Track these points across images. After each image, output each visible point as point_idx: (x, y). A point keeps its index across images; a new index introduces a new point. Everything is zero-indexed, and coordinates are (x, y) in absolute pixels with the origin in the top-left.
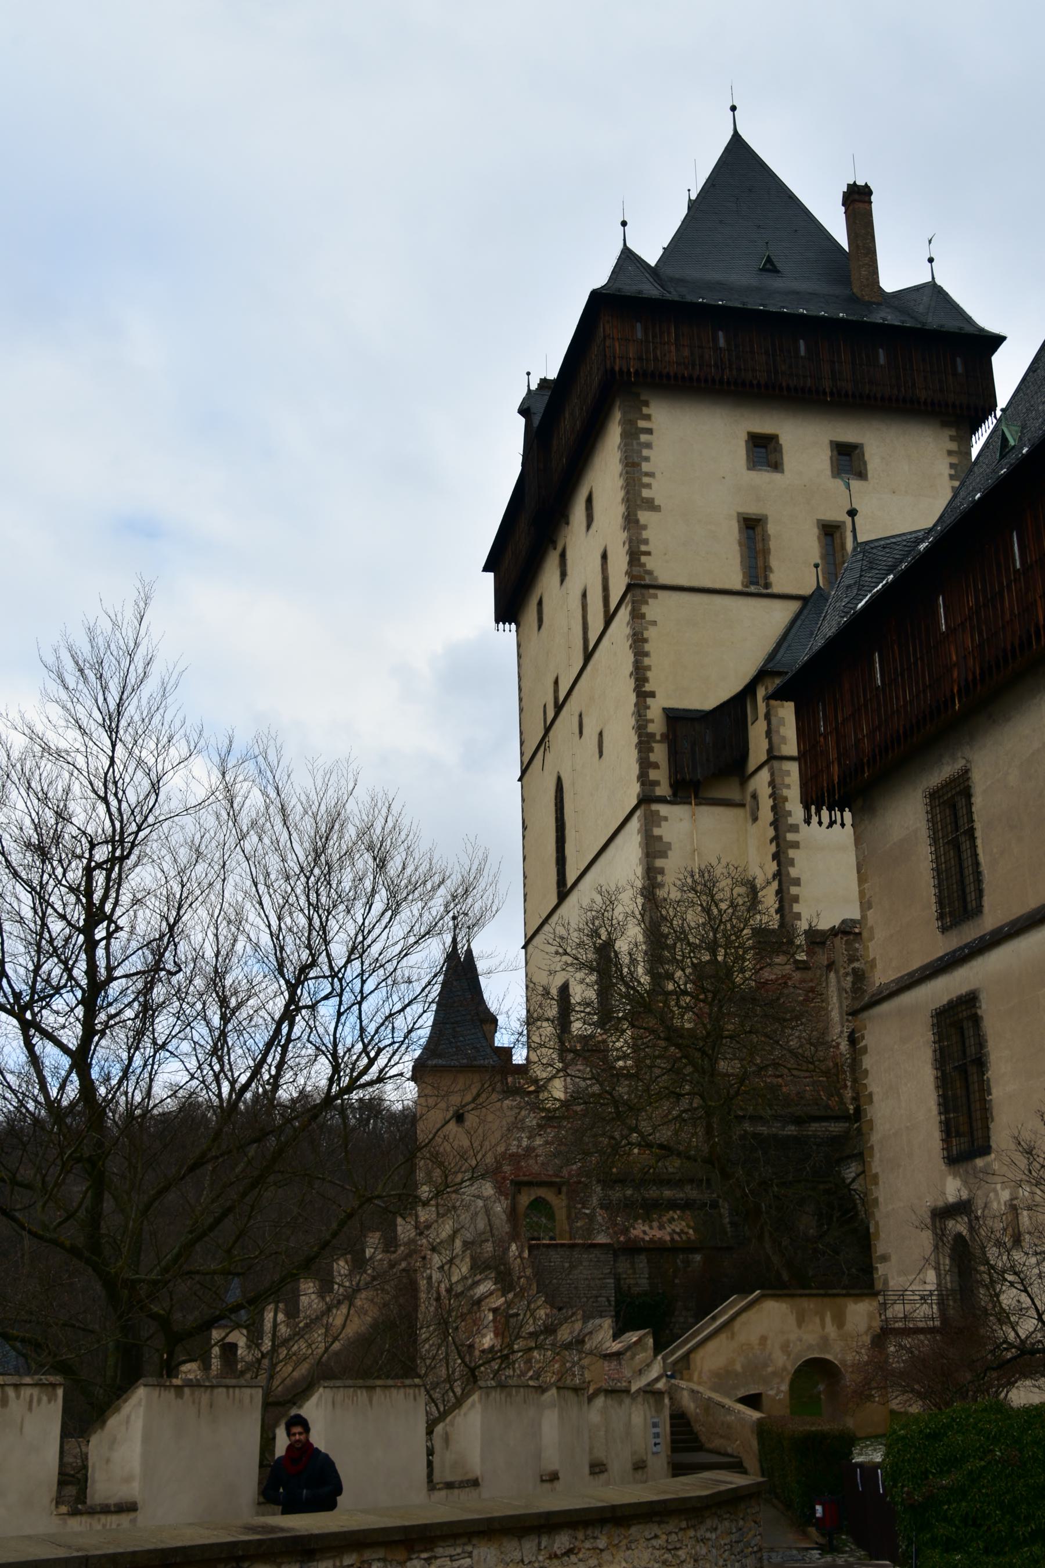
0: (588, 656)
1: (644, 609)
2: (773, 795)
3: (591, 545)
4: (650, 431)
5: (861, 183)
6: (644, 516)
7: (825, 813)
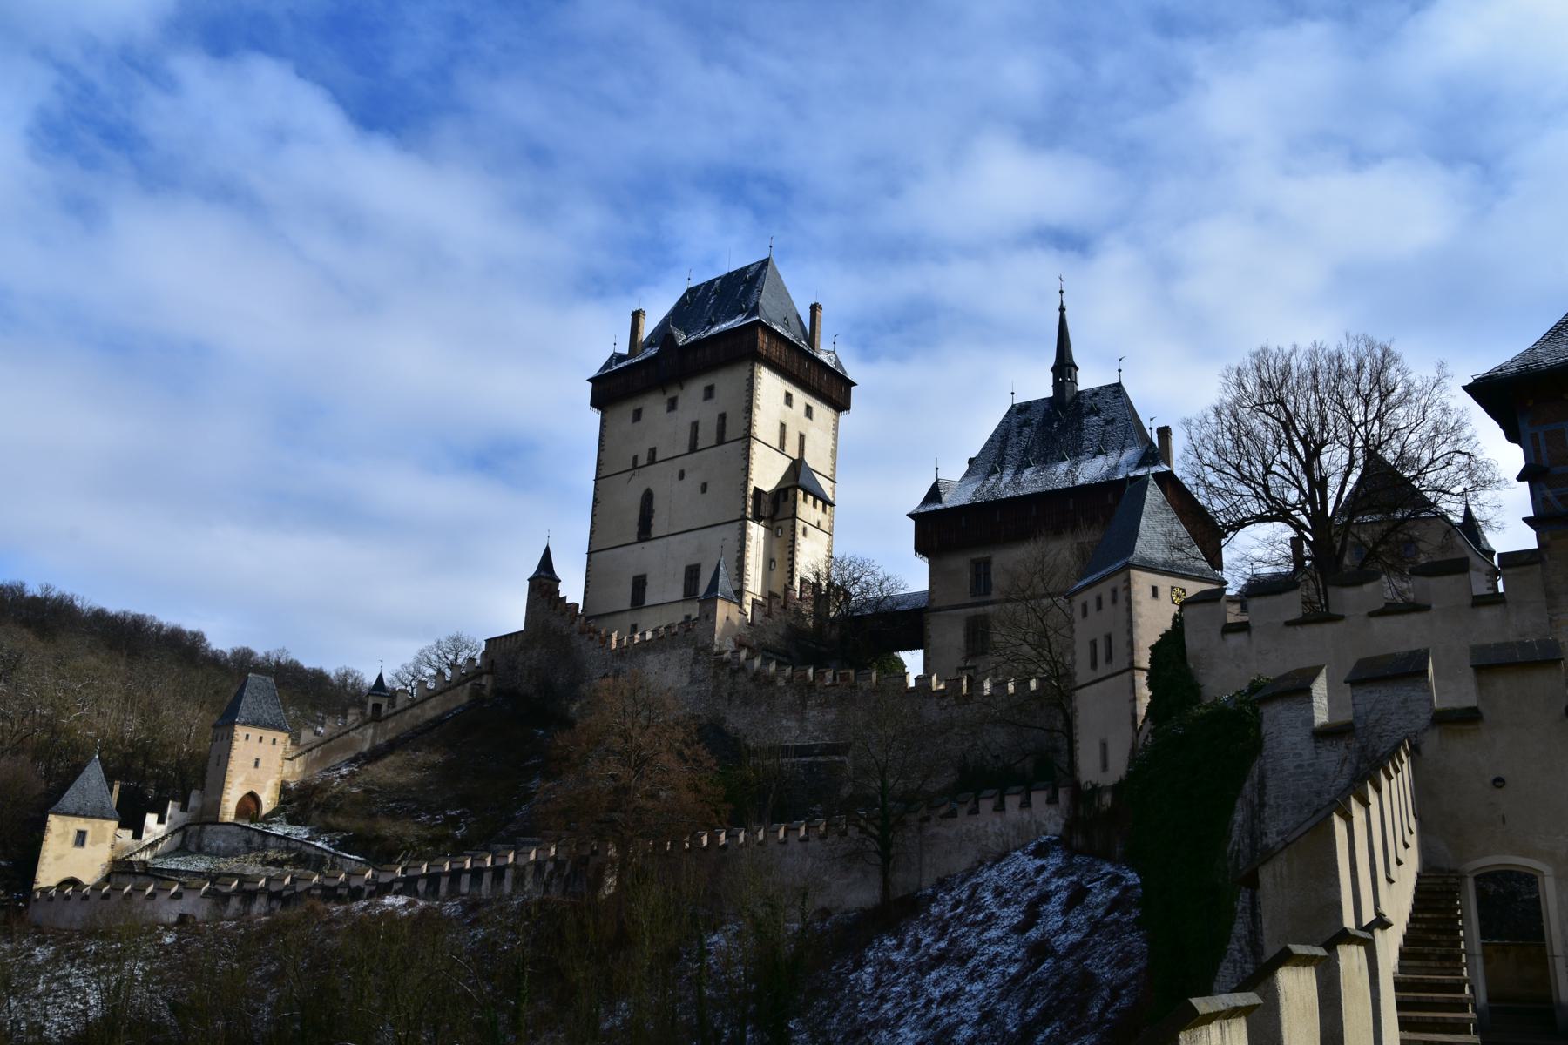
0: (693, 448)
6: (756, 411)
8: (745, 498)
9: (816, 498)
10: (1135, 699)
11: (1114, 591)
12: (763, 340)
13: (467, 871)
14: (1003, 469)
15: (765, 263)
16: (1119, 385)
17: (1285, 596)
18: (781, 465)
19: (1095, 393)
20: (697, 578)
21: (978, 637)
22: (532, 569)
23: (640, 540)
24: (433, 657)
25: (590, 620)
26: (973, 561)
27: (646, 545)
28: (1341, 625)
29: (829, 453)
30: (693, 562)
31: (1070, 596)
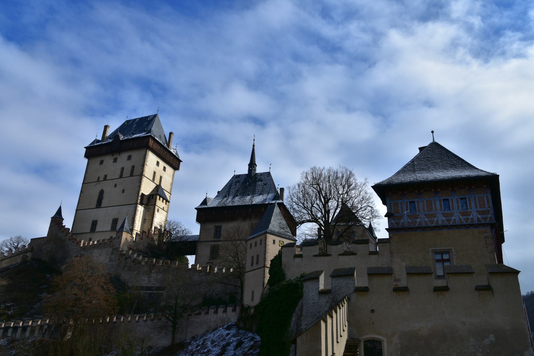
0: (121, 177)
6: (146, 166)
8: (138, 196)
9: (163, 199)
10: (264, 277)
11: (261, 240)
12: (151, 142)
13: (12, 328)
14: (229, 196)
15: (155, 116)
16: (269, 173)
17: (314, 247)
18: (153, 186)
19: (261, 174)
20: (117, 223)
21: (214, 253)
22: (53, 213)
23: (97, 207)
24: (8, 244)
25: (73, 235)
26: (215, 226)
27: (99, 209)
28: (330, 257)
29: (170, 184)
30: (116, 217)
31: (246, 241)
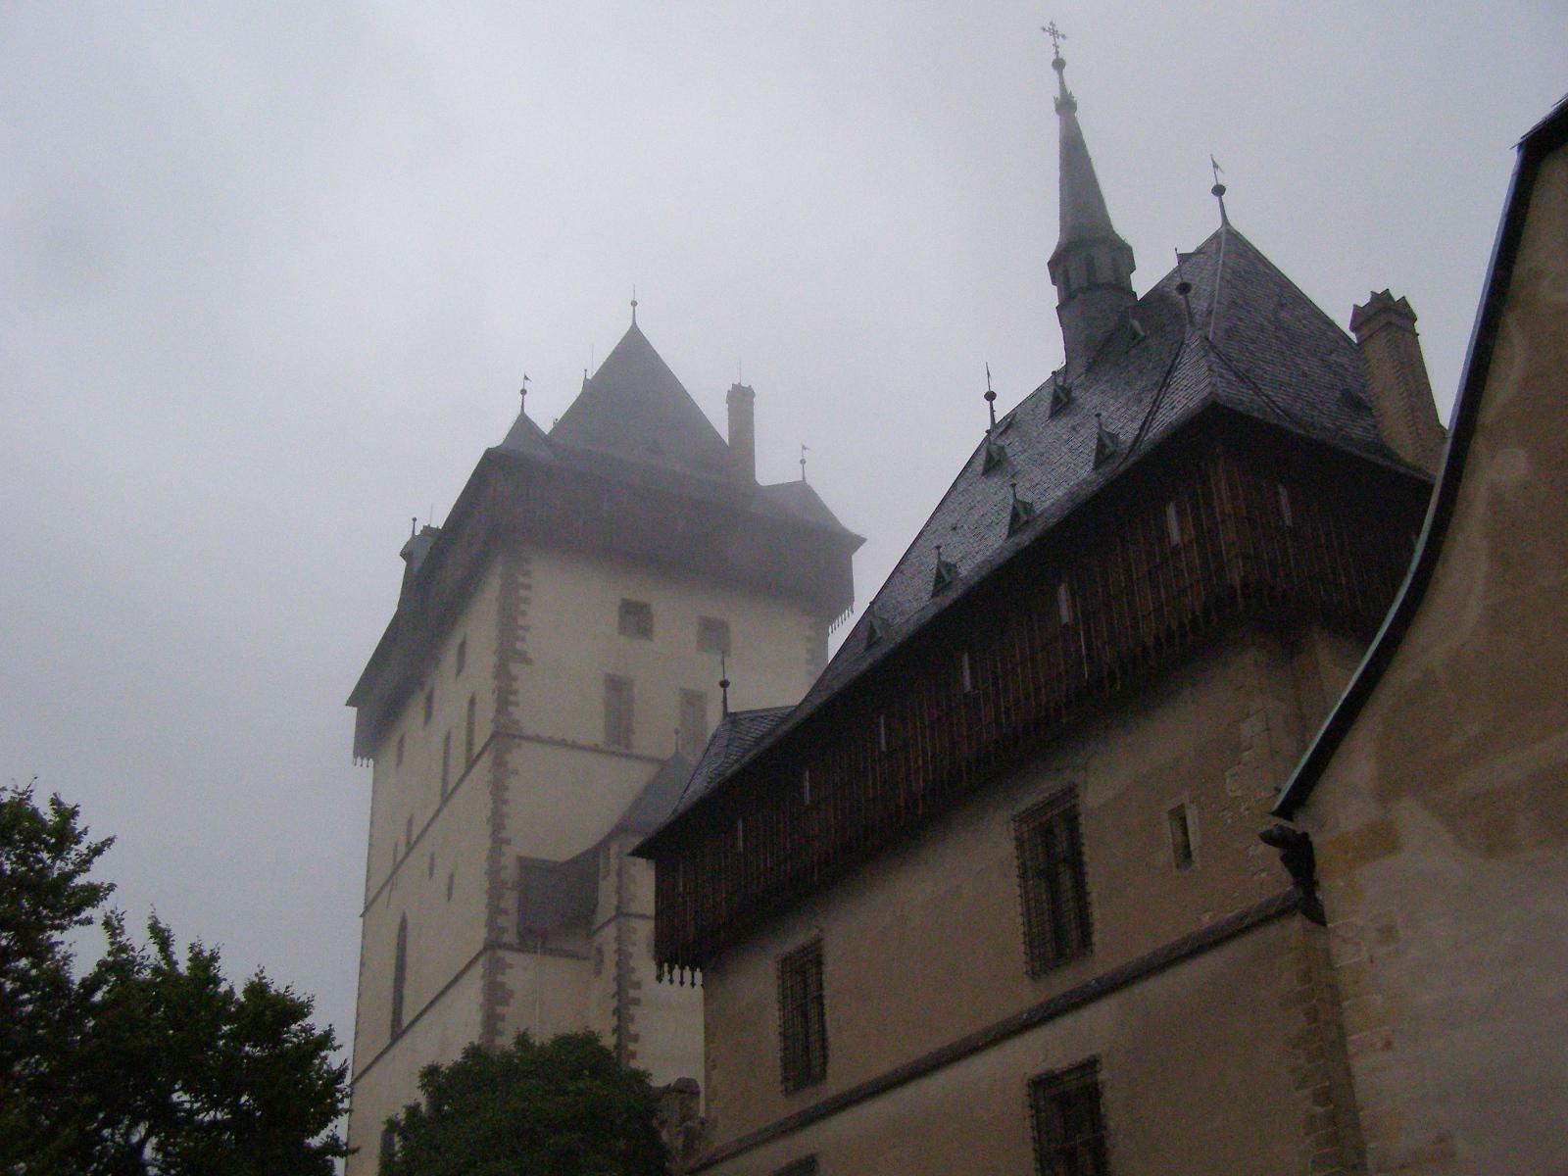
0: (446, 798)
1: (508, 757)
2: (619, 951)
3: (460, 688)
4: (529, 587)
5: (745, 384)
6: (516, 668)
7: (677, 971)
